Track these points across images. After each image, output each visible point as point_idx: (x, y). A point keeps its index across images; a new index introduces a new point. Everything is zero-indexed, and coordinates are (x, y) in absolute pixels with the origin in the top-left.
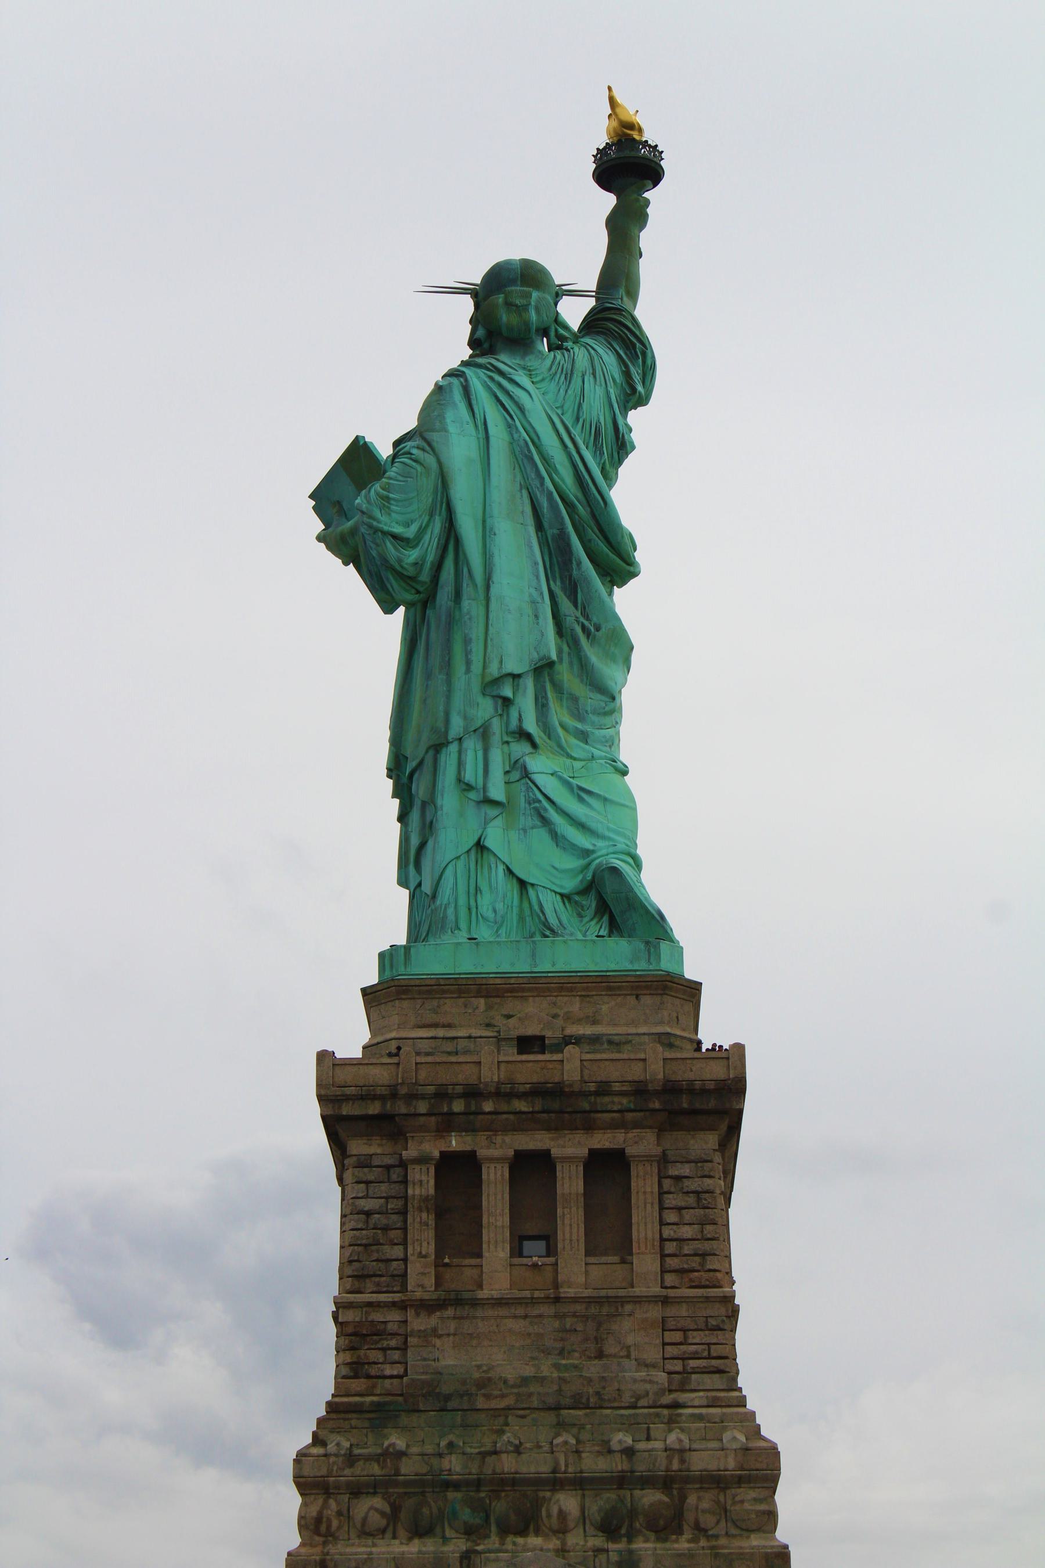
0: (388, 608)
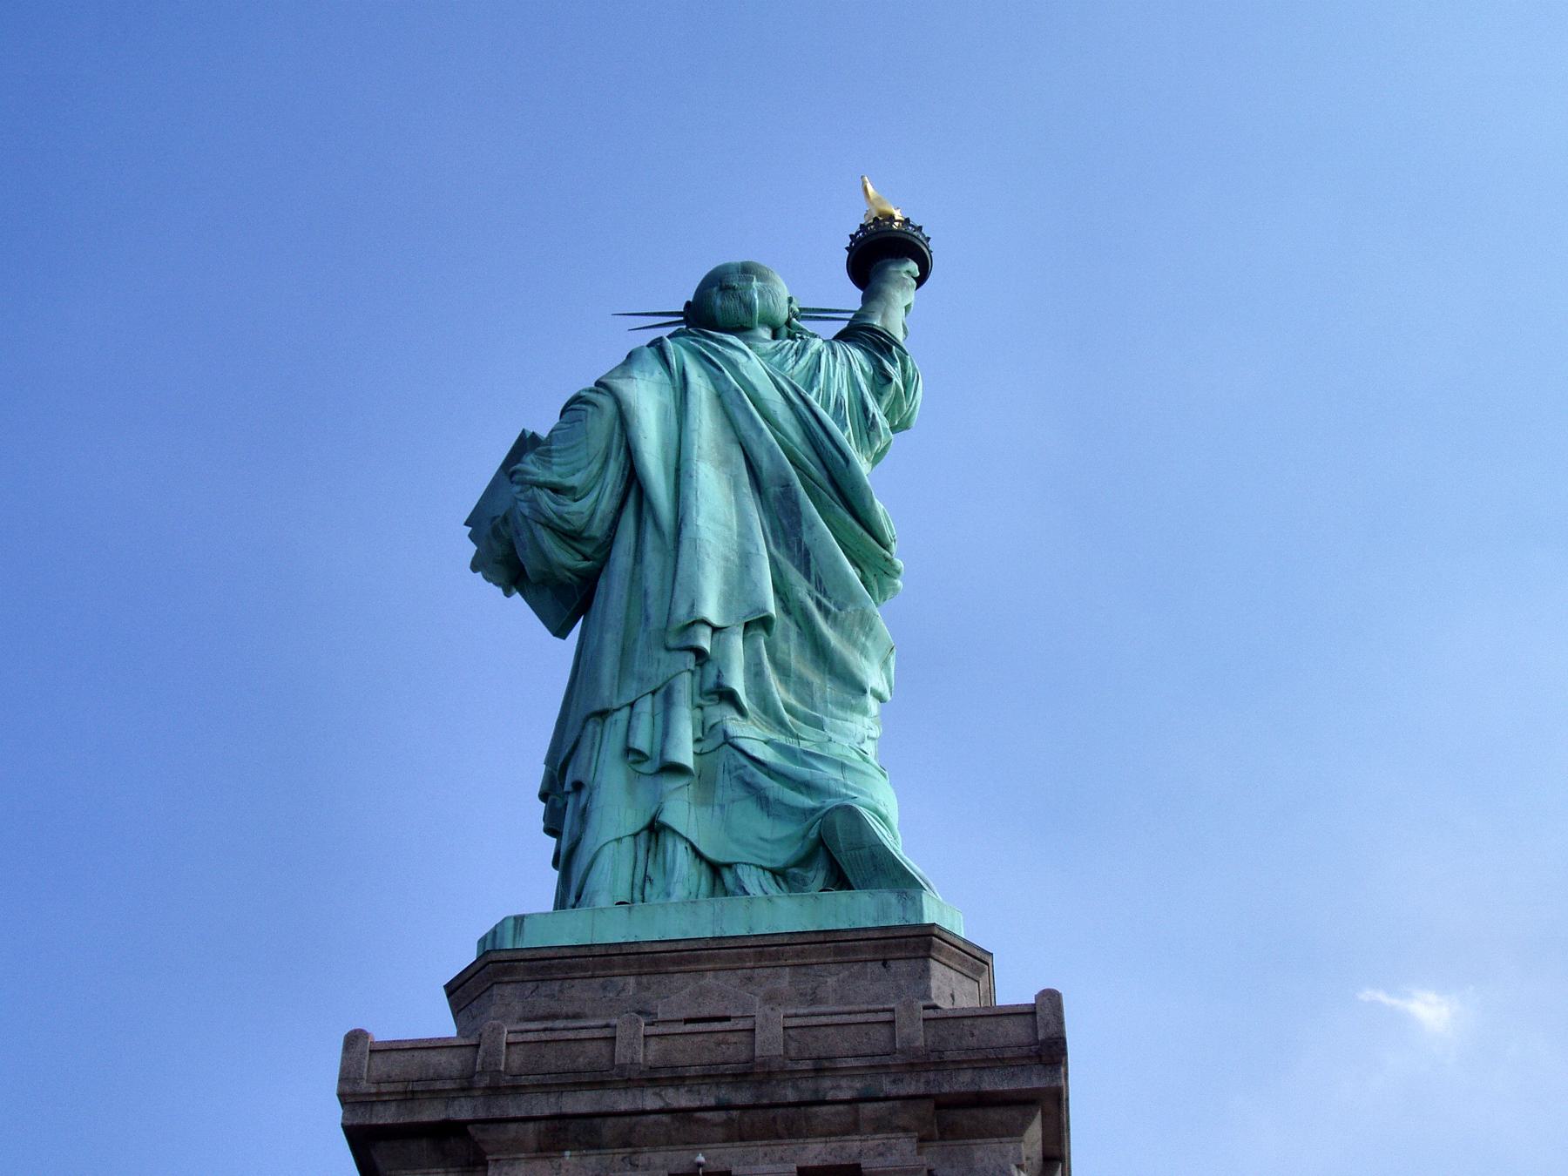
0: (561, 632)
